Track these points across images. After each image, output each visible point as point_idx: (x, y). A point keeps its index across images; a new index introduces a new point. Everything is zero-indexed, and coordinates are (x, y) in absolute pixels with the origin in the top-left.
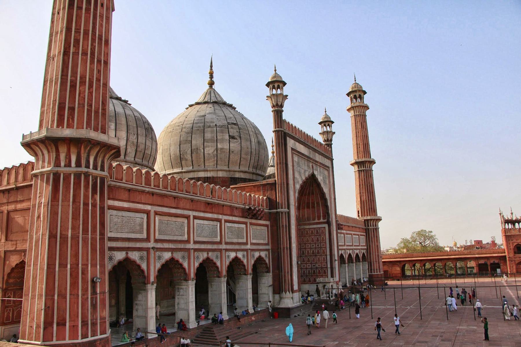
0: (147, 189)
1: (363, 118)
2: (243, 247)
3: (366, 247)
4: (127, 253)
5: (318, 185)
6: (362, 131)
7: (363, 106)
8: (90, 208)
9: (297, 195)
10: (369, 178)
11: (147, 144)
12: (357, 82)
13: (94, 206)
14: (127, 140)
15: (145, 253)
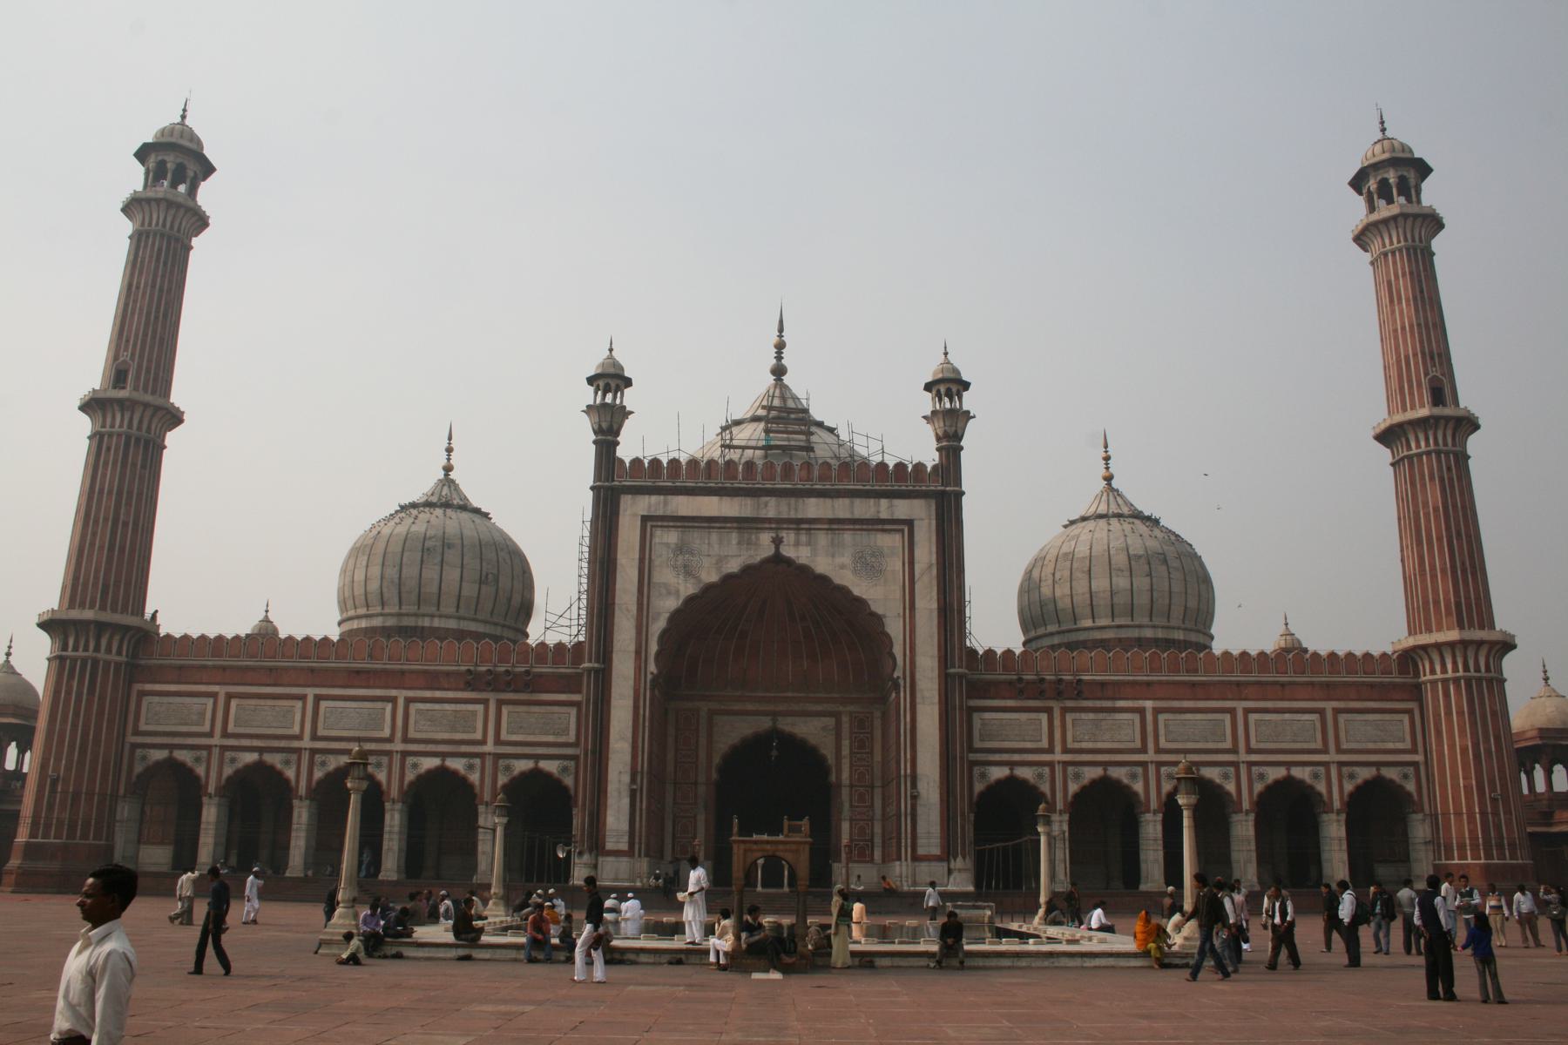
0: (210, 663)
1: (1395, 263)
2: (464, 749)
3: (1419, 758)
4: (171, 753)
5: (824, 579)
6: (1393, 312)
7: (1416, 216)
8: (63, 695)
9: (658, 626)
10: (1423, 485)
11: (423, 575)
12: (1389, 134)
13: (69, 693)
14: (382, 578)
15: (204, 753)
